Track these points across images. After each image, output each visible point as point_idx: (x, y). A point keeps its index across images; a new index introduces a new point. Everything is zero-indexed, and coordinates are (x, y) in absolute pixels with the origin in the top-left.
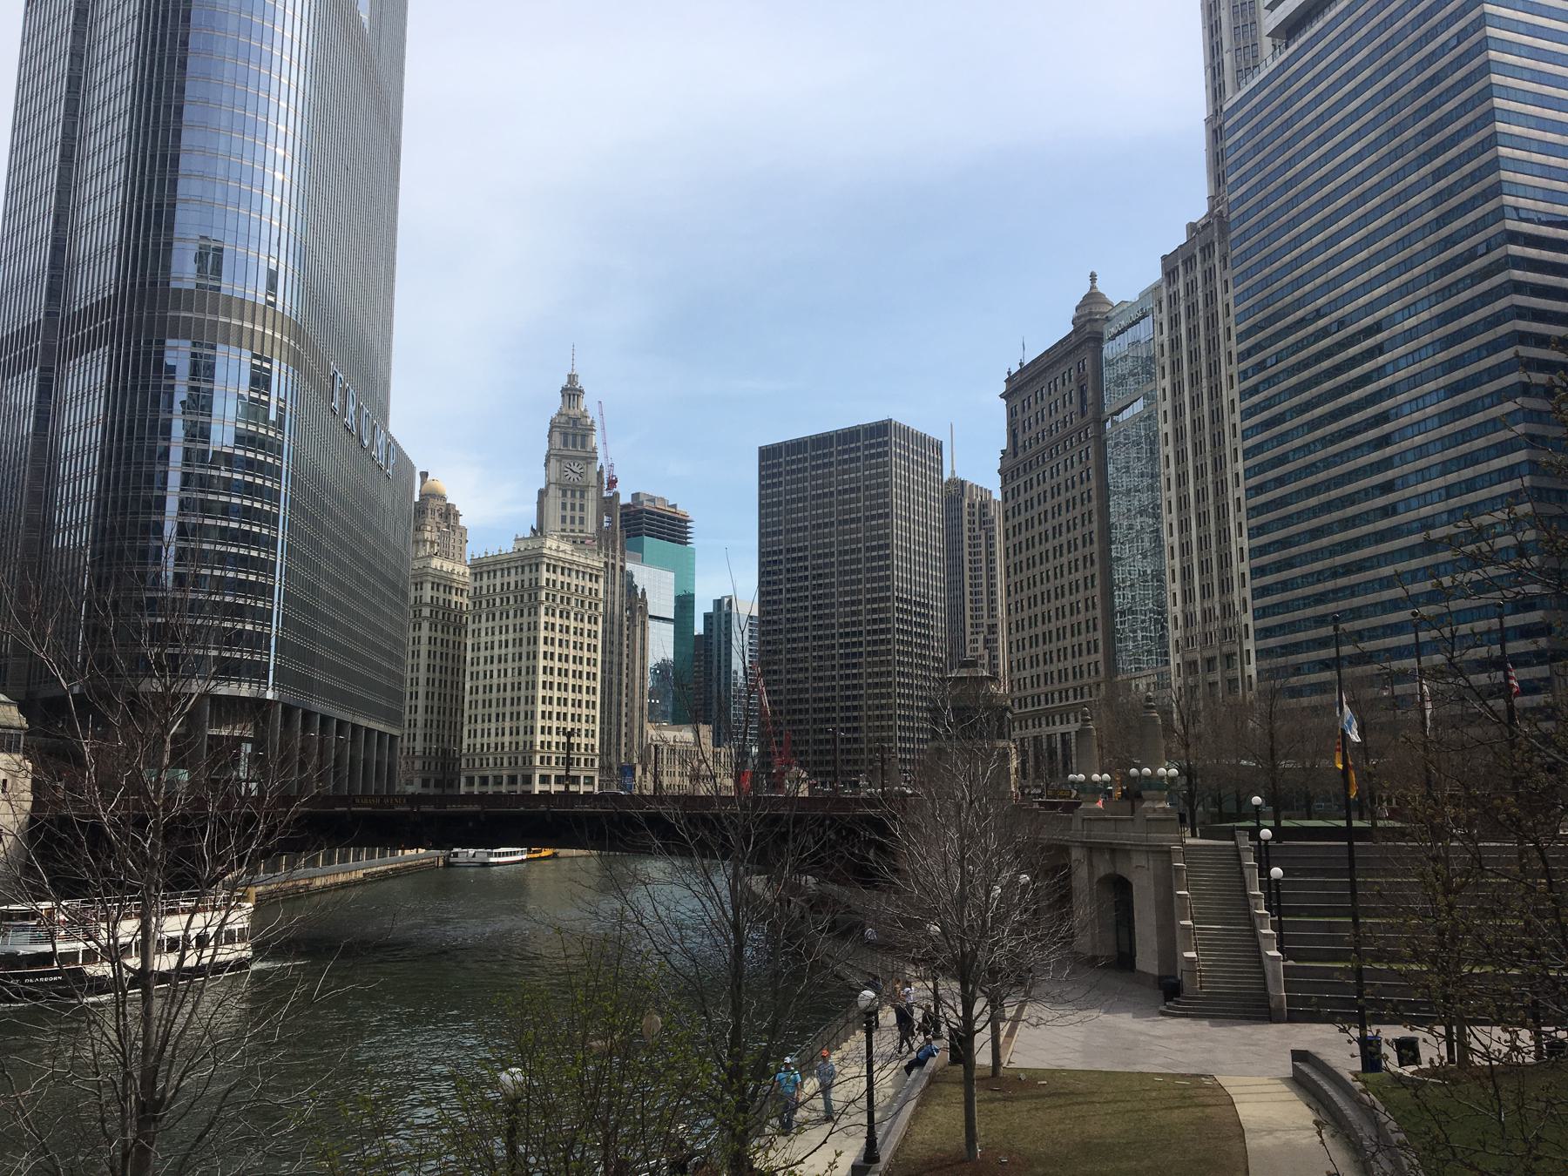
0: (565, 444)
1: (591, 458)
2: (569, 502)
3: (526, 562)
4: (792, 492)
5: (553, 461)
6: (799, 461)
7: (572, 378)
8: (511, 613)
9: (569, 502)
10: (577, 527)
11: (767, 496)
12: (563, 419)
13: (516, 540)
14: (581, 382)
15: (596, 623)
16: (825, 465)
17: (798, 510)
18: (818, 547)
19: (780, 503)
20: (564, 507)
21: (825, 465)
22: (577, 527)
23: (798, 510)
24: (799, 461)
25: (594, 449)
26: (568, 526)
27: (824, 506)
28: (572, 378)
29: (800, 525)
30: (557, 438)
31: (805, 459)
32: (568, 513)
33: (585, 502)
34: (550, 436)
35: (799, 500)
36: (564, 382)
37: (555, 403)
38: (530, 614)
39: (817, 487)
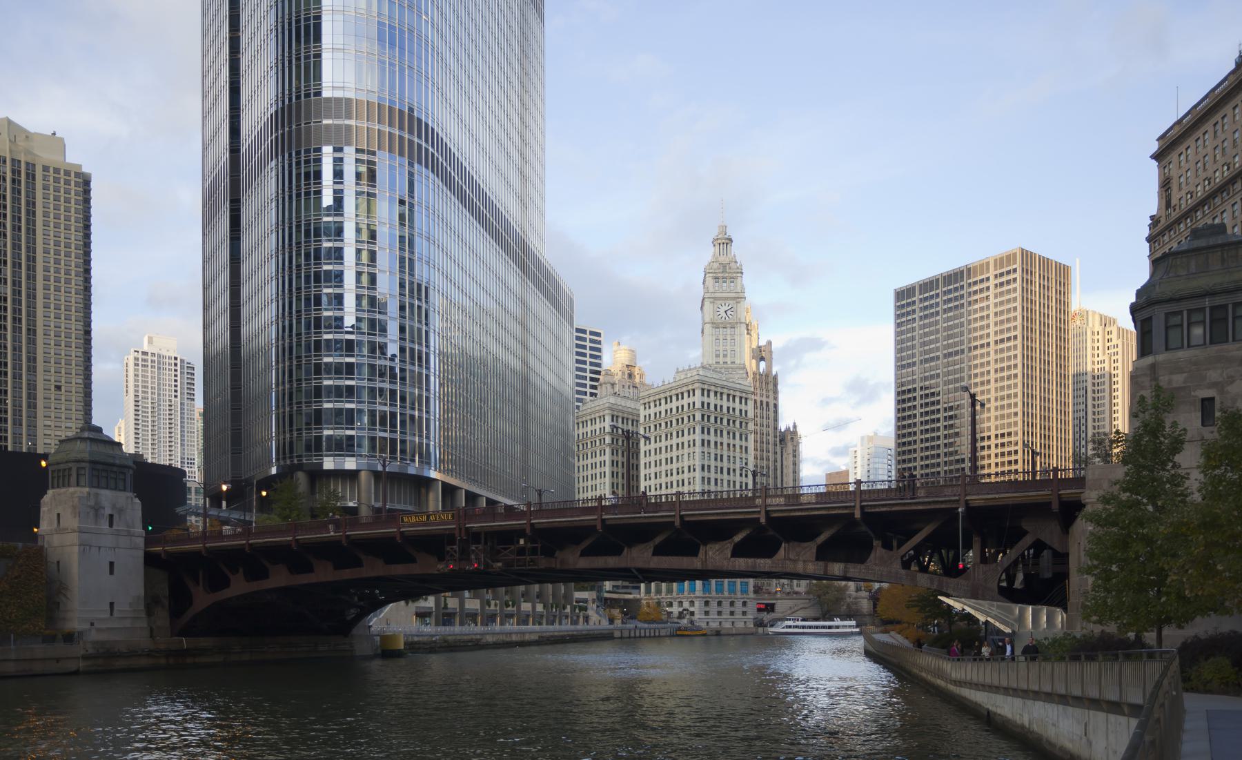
1: (739, 298)
4: (924, 326)
5: (707, 303)
6: (932, 297)
7: (723, 229)
8: (674, 434)
12: (716, 265)
13: (678, 372)
14: (730, 233)
16: (956, 299)
17: (931, 342)
18: (949, 373)
19: (913, 338)
21: (956, 299)
23: (931, 342)
24: (932, 297)
25: (743, 288)
27: (954, 336)
28: (723, 229)
29: (932, 355)
30: (710, 281)
31: (937, 295)
35: (931, 333)
36: (714, 233)
37: (707, 254)
38: (689, 434)
39: (949, 319)
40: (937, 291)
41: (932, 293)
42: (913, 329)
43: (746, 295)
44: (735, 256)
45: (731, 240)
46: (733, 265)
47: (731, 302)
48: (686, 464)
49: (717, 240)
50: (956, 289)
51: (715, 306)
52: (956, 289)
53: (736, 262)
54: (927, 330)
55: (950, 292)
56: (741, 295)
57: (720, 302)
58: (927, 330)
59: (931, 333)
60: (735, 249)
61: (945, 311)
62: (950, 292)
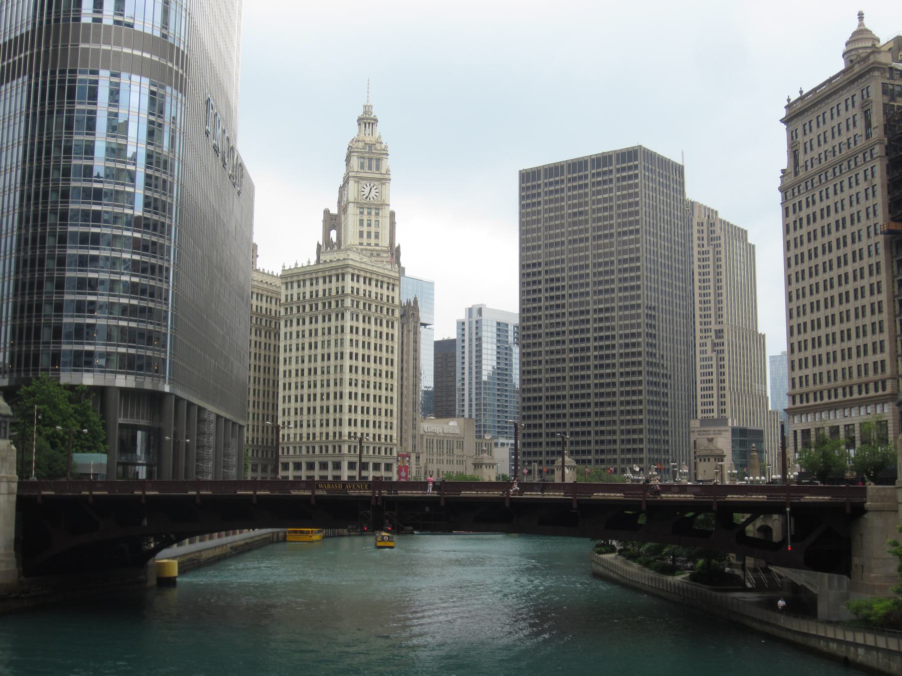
0: (362, 166)
2: (365, 218)
3: (334, 272)
5: (352, 183)
7: (367, 109)
9: (365, 218)
10: (373, 241)
11: (528, 214)
14: (375, 113)
15: (392, 327)
18: (575, 259)
20: (361, 222)
22: (373, 241)
24: (557, 182)
25: (388, 171)
26: (365, 240)
28: (367, 109)
30: (355, 162)
32: (365, 229)
33: (380, 219)
34: (348, 160)
35: (557, 218)
36: (360, 113)
37: (353, 131)
40: (562, 178)
41: (557, 179)
42: (539, 212)
43: (391, 177)
44: (380, 137)
45: (376, 120)
46: (378, 146)
47: (376, 183)
48: (332, 351)
49: (363, 119)
50: (580, 178)
51: (360, 186)
52: (580, 178)
53: (381, 143)
54: (552, 214)
55: (574, 179)
56: (386, 177)
57: (365, 182)
58: (552, 214)
59: (557, 218)
60: (379, 129)
61: (569, 198)
62: (574, 179)
